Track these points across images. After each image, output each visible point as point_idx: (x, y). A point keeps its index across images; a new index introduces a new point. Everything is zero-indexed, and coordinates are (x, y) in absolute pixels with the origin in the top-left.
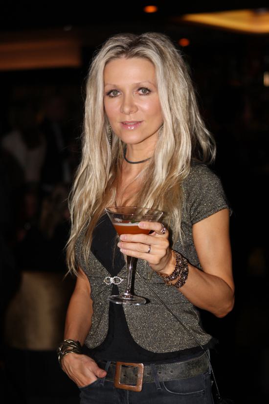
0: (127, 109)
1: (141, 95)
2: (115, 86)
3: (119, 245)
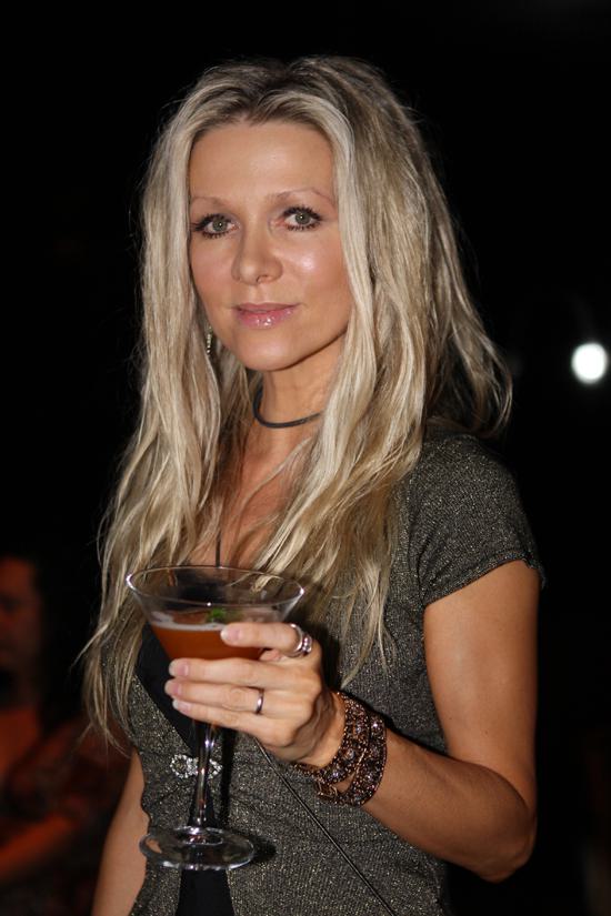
0: (249, 270)
1: (291, 228)
2: (216, 202)
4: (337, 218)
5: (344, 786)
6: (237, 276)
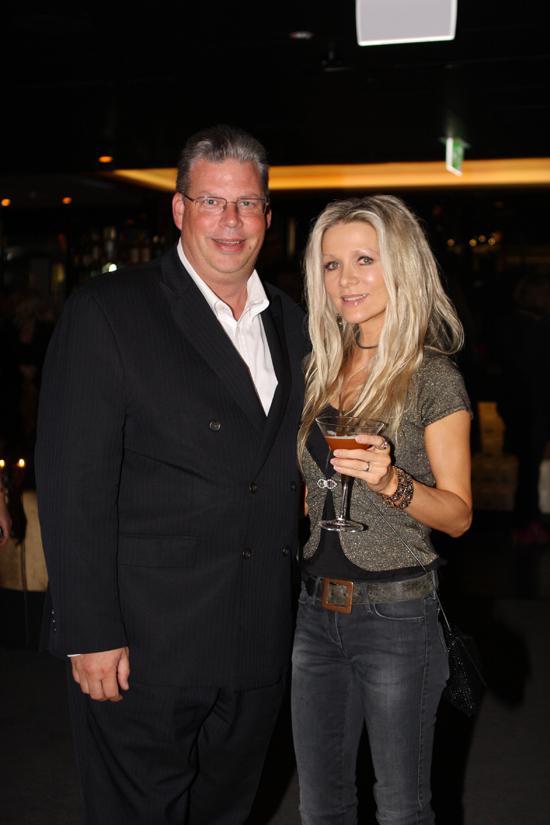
0: (344, 282)
2: (331, 256)
3: (332, 461)
4: (380, 260)
5: (398, 503)
6: (340, 285)
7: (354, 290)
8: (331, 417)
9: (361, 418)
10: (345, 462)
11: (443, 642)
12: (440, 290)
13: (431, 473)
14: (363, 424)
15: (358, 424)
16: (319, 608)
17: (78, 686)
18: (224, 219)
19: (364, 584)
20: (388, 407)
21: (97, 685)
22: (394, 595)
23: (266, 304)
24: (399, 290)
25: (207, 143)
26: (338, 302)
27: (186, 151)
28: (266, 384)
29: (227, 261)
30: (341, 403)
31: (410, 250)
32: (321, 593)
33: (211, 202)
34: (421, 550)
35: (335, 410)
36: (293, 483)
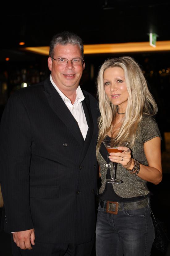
0: (112, 90)
1: (118, 83)
2: (107, 80)
3: (109, 157)
4: (125, 81)
7: (116, 93)
8: (109, 140)
9: (119, 141)
10: (114, 157)
11: (153, 224)
12: (148, 92)
13: (146, 161)
14: (120, 143)
15: (118, 143)
16: (105, 212)
17: (16, 244)
18: (67, 66)
19: (122, 203)
20: (130, 136)
21: (23, 244)
22: (134, 207)
23: (83, 98)
24: (133, 92)
25: (60, 38)
26: (110, 97)
27: (52, 41)
28: (84, 128)
29: (69, 82)
30: (112, 135)
31: (137, 77)
32: (106, 207)
33: (62, 60)
34: (143, 189)
35: (110, 138)
36: (95, 165)
